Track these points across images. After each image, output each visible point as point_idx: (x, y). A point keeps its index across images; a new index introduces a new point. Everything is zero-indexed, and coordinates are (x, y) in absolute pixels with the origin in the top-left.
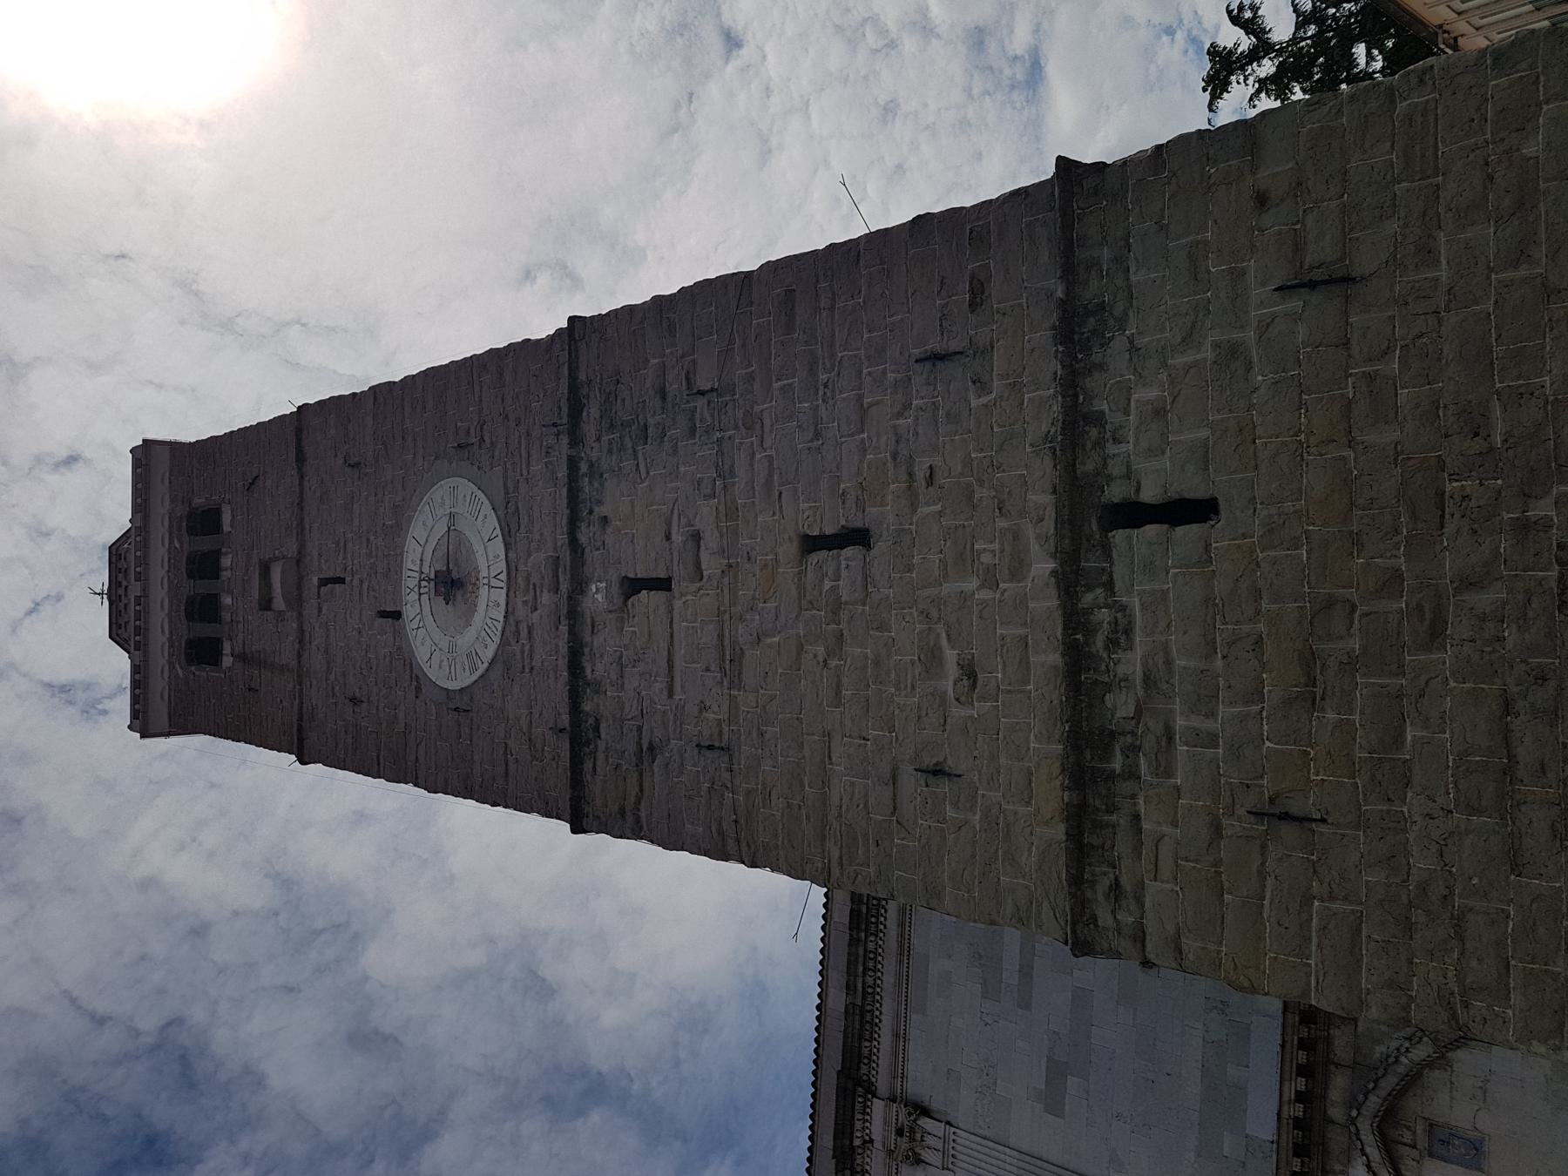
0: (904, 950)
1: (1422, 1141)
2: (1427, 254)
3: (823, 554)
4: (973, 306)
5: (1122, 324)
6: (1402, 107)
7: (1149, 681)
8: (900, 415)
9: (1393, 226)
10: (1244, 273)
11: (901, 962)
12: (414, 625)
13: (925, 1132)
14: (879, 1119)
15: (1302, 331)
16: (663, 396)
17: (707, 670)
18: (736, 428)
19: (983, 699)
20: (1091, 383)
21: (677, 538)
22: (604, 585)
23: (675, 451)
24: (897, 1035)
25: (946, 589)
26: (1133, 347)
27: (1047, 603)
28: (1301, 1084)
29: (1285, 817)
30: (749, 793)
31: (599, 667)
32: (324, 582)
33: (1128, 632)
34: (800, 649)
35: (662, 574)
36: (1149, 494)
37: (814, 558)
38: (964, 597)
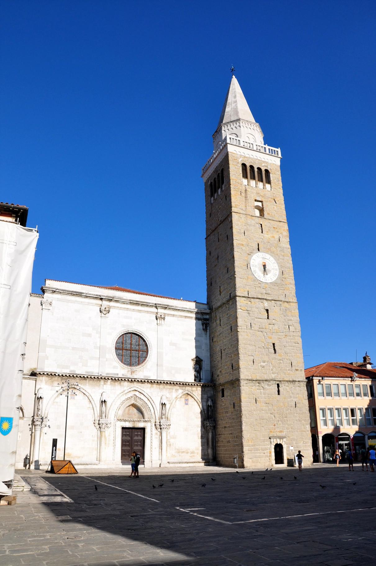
0: (186, 317)
1: (186, 398)
2: (297, 414)
3: (273, 346)
4: (296, 369)
5: (294, 387)
6: (307, 412)
7: (265, 388)
8: (287, 359)
9: (299, 411)
10: (297, 398)
11: (184, 316)
12: (258, 256)
13: (161, 320)
14: (161, 311)
15: (292, 403)
16: (289, 320)
17: (259, 326)
18: (285, 333)
19: (261, 368)
20: (289, 382)
21: (274, 321)
22: (267, 305)
23: (283, 322)
24: (174, 315)
25: (271, 364)
26: (292, 387)
27: (271, 378)
28: (190, 384)
29: (256, 401)
30: (247, 332)
31: (257, 303)
32: (261, 225)
33: (269, 386)
34: (263, 342)
35: (269, 318)
36: (280, 388)
37: (272, 345)
38: (270, 367)
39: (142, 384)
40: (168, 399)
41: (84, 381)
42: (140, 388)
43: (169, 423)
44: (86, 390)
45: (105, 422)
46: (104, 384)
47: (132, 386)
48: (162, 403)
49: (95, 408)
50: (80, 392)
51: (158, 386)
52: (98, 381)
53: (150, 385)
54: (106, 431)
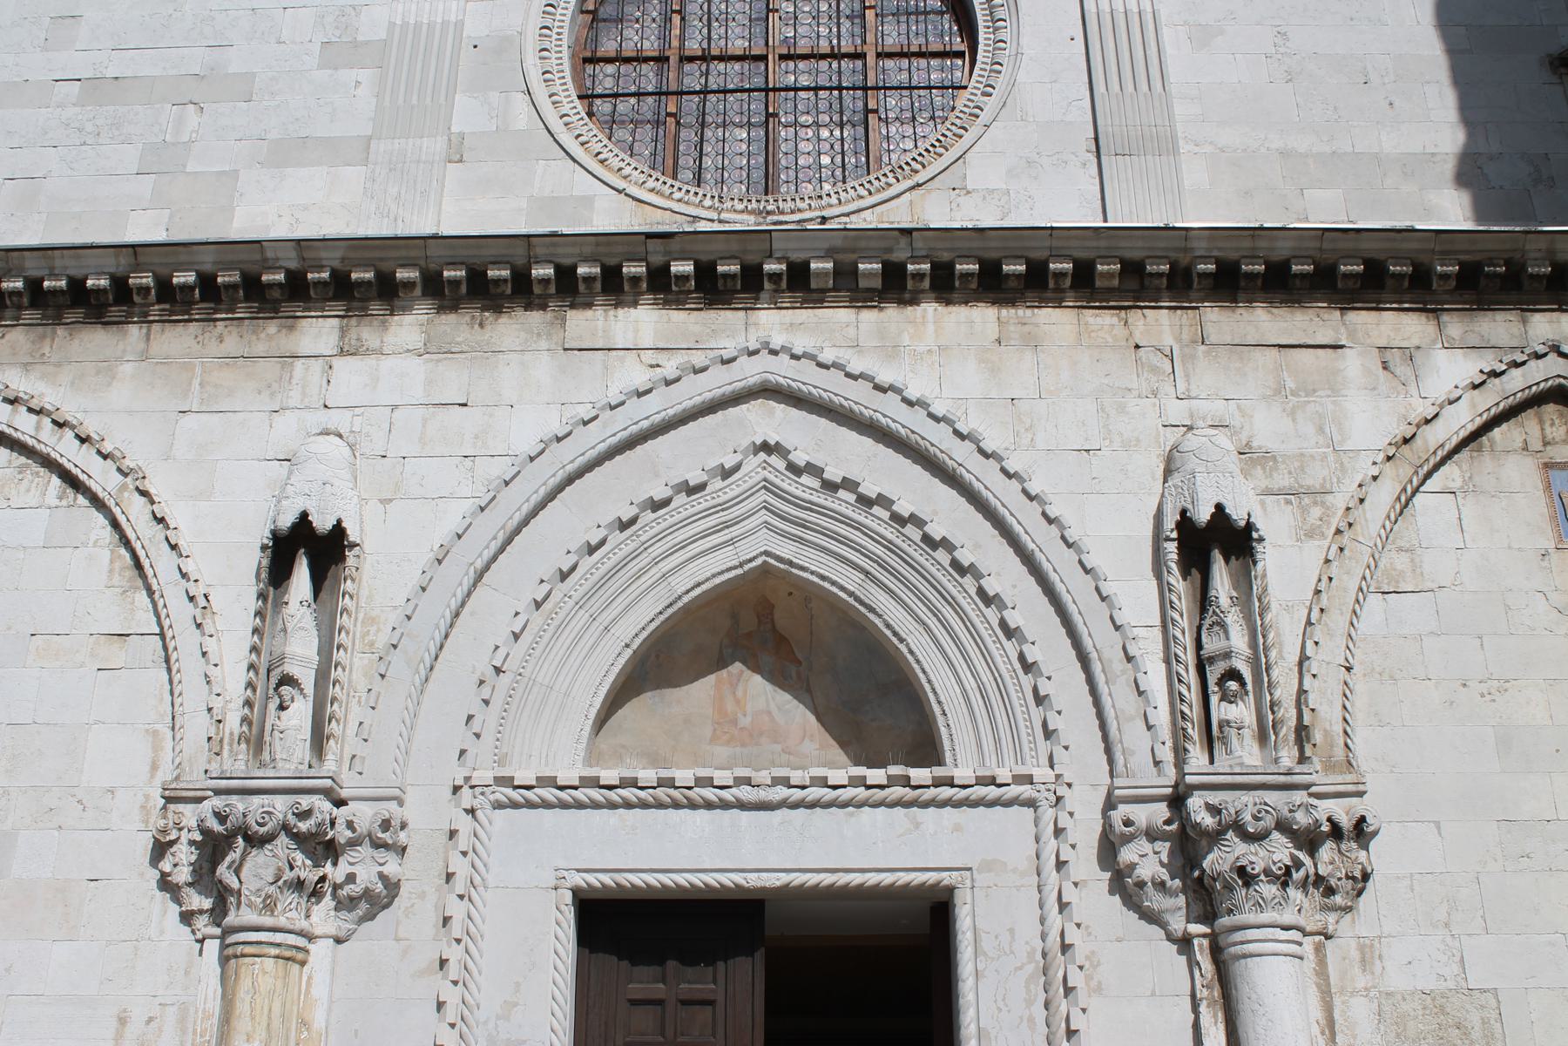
39: (869, 316)
40: (1282, 480)
41: (94, 341)
42: (827, 356)
43: (1344, 813)
44: (91, 428)
45: (281, 806)
46: (342, 352)
47: (729, 346)
48: (1185, 523)
49: (185, 641)
50: (21, 469)
51: (1103, 322)
52: (272, 327)
53: (982, 318)
54: (320, 952)
